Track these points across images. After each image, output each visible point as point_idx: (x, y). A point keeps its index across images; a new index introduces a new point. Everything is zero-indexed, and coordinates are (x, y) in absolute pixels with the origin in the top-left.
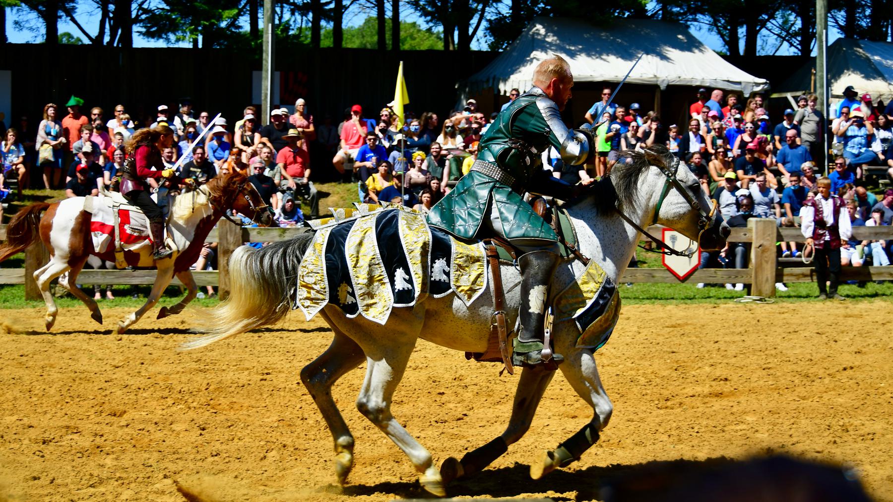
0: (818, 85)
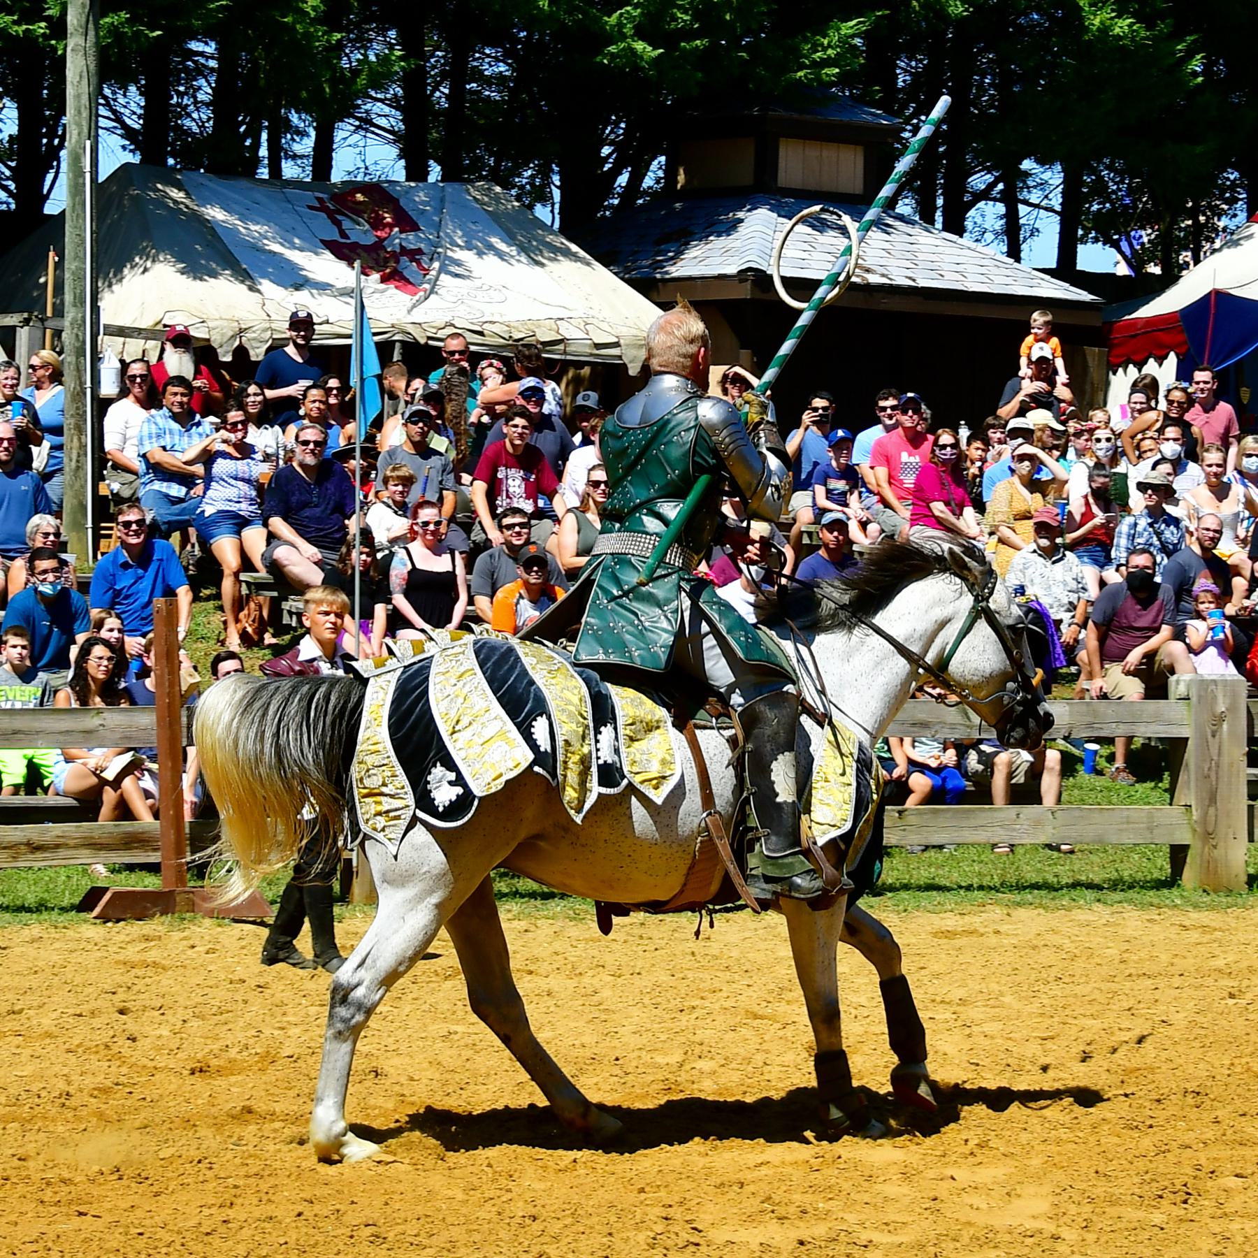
0: (68, 297)
